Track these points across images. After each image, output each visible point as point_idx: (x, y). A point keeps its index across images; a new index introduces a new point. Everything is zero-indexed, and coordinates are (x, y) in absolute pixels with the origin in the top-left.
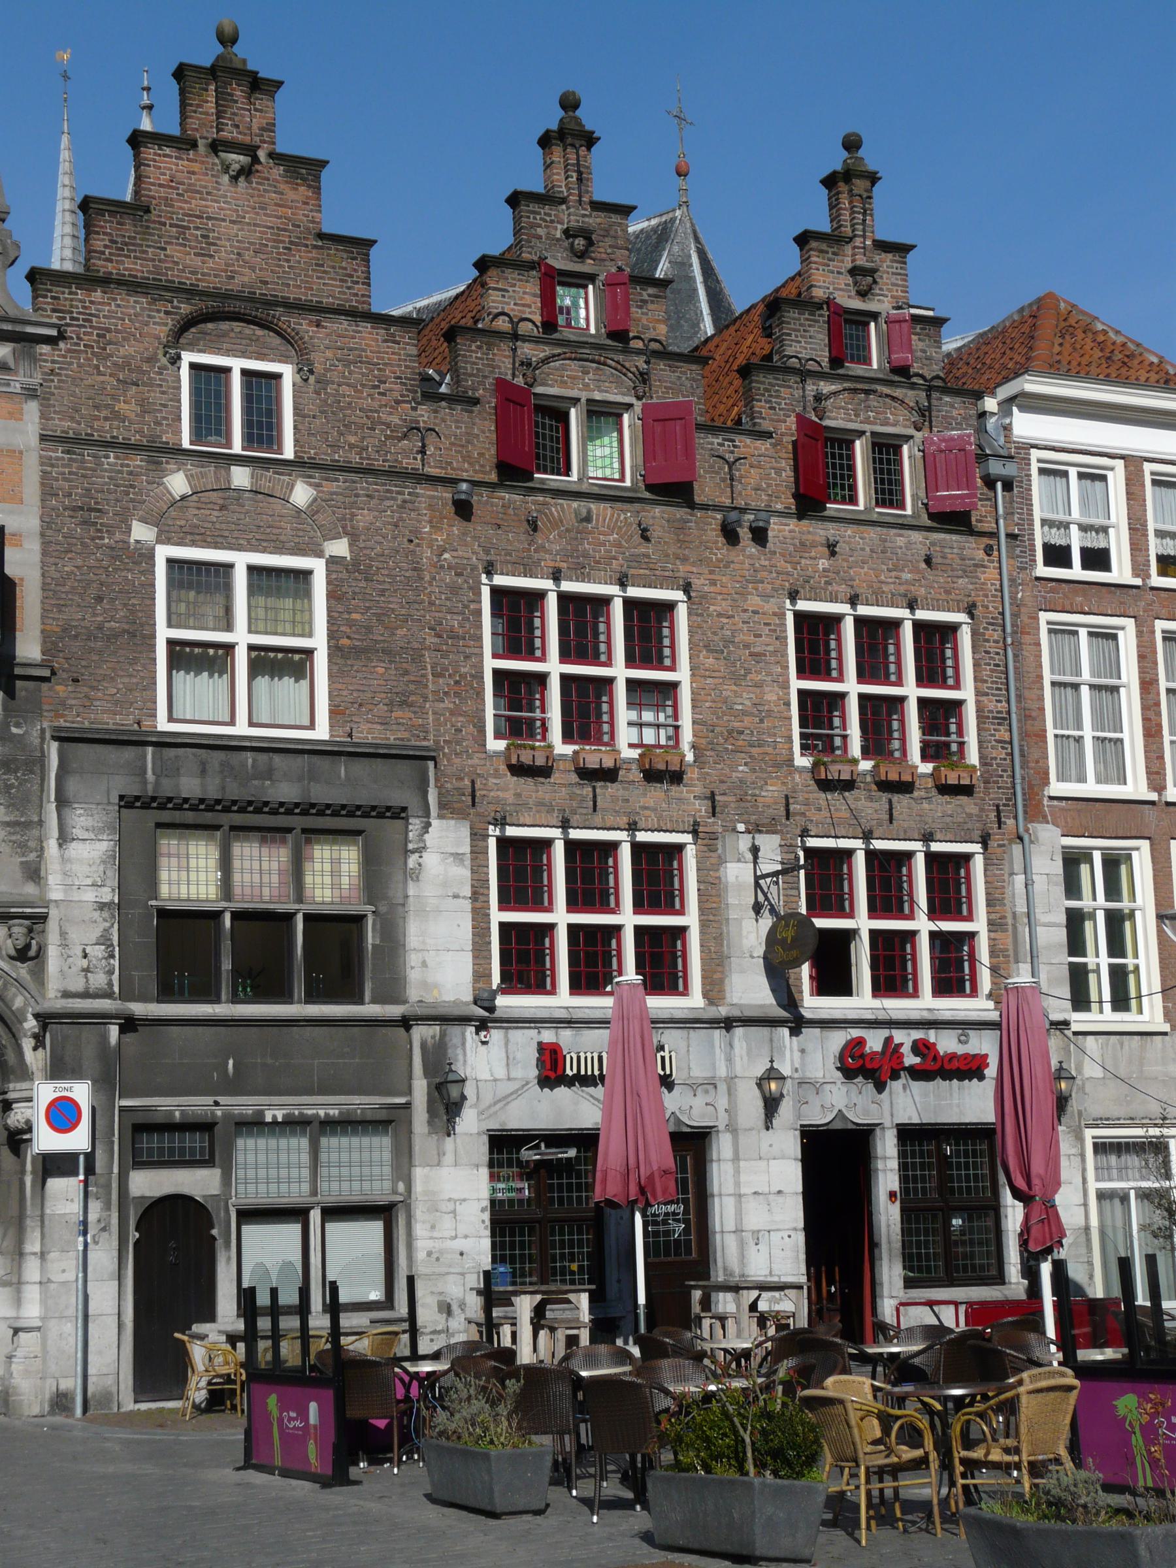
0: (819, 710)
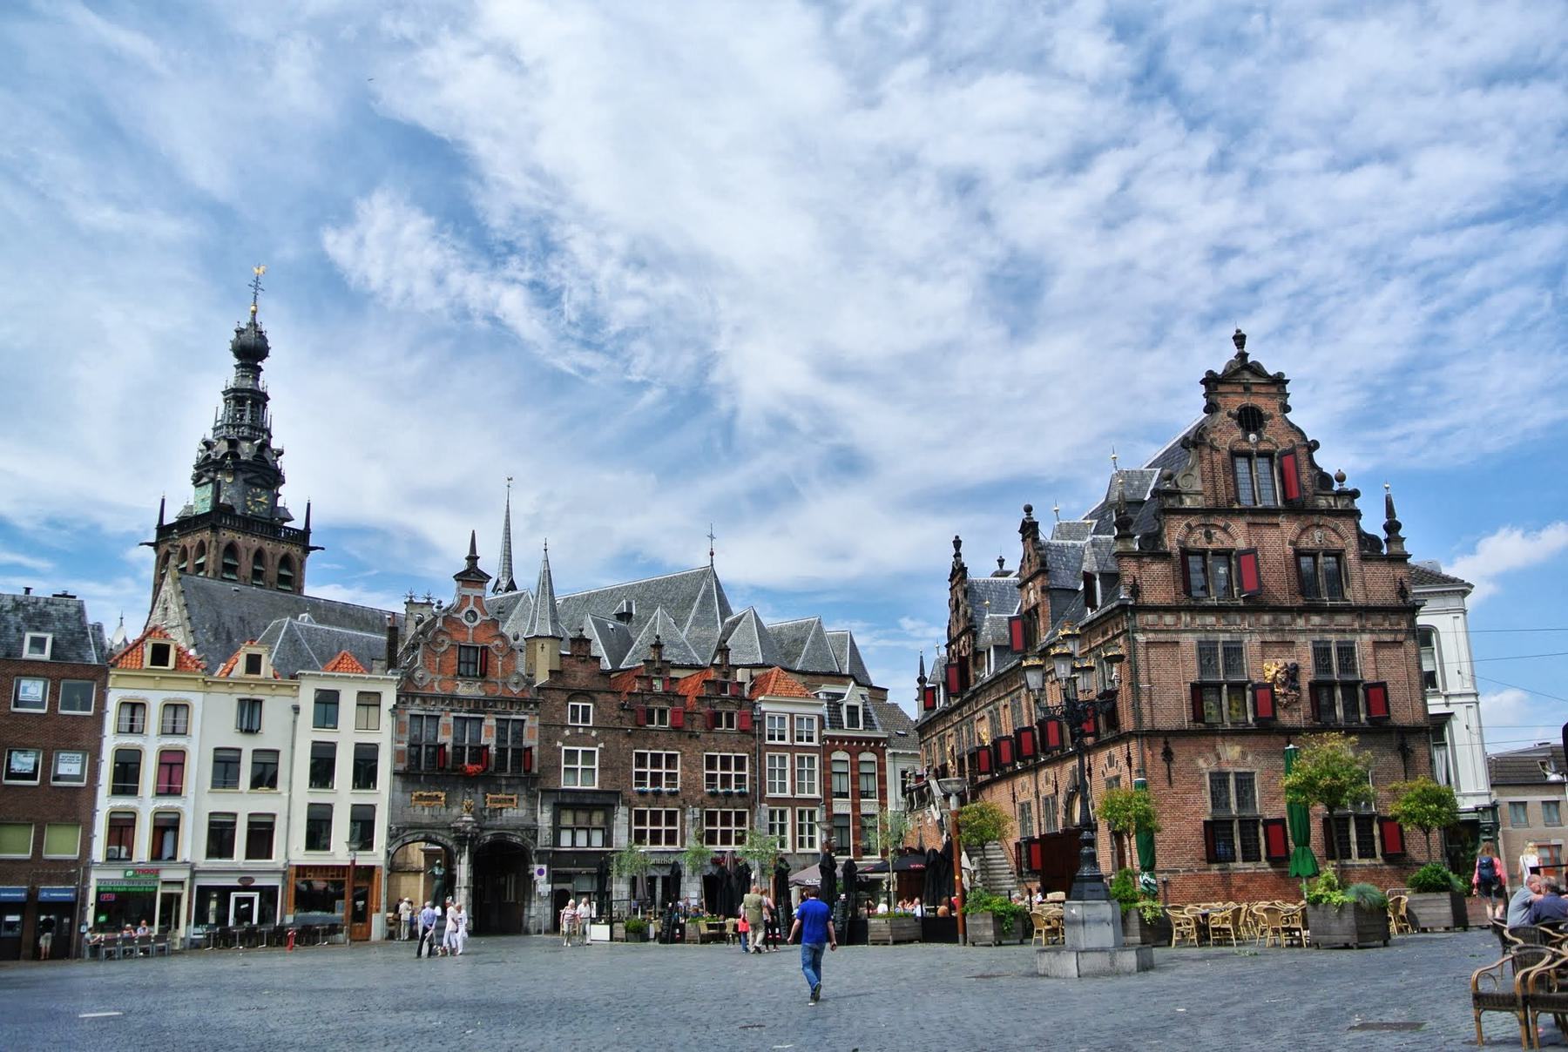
0: (711, 778)
